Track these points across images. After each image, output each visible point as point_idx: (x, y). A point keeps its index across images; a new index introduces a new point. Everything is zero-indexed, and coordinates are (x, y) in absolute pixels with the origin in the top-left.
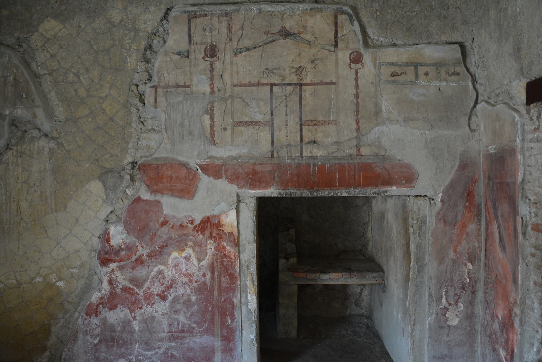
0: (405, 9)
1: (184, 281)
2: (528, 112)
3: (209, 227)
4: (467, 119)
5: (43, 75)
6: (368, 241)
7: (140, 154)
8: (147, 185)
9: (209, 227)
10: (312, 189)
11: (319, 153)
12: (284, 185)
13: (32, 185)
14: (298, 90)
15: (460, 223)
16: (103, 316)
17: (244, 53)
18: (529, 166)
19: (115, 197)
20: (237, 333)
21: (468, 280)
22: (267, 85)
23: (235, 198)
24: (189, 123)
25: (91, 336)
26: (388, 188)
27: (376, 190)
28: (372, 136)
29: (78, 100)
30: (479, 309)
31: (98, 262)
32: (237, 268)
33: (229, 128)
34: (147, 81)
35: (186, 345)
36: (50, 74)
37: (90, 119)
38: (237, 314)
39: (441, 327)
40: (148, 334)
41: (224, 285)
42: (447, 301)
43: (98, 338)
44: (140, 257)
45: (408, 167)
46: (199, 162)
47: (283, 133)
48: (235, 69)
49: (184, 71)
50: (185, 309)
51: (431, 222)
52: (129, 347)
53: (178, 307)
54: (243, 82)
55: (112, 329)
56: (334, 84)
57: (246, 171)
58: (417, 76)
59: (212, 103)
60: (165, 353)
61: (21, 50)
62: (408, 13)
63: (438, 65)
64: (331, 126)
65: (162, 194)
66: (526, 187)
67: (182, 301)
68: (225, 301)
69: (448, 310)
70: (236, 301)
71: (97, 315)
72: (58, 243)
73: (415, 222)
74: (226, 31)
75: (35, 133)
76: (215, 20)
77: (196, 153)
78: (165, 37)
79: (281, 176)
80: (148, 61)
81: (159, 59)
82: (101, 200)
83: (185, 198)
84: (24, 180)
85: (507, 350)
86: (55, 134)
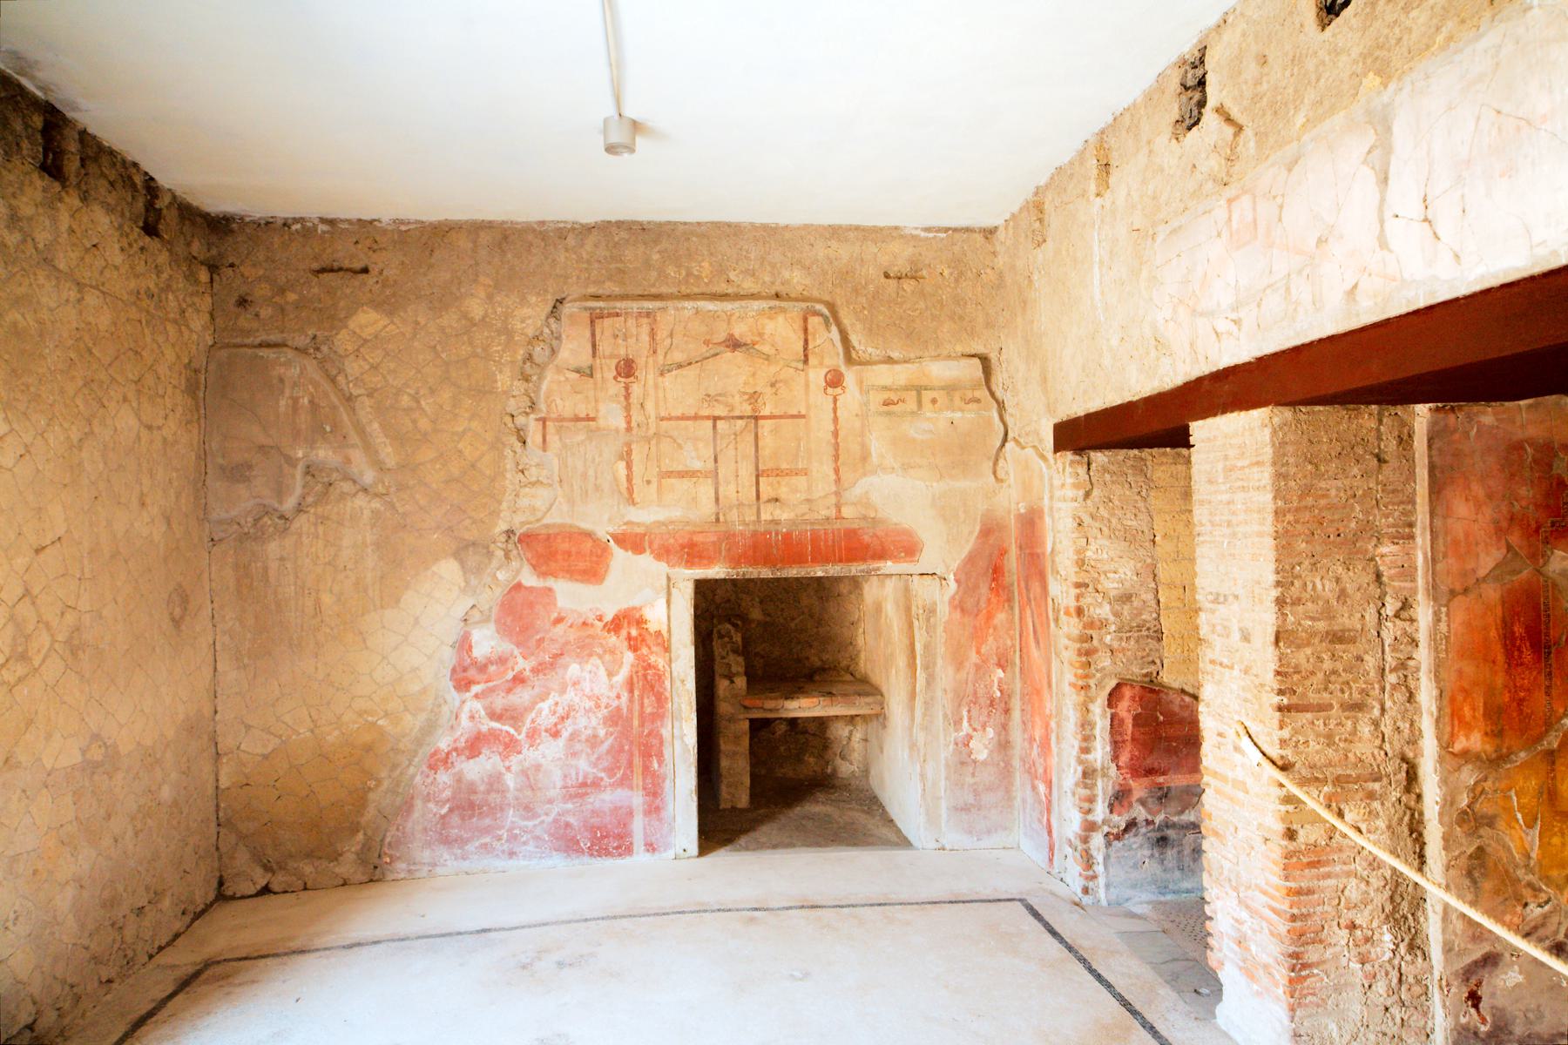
0: (904, 307)
1: (587, 707)
2: (1055, 460)
3: (626, 625)
4: (991, 464)
5: (360, 396)
6: (859, 651)
7: (518, 519)
8: (531, 564)
9: (626, 625)
10: (775, 566)
11: (784, 515)
12: (736, 561)
13: (341, 567)
14: (753, 425)
15: (984, 611)
16: (457, 769)
17: (674, 372)
18: (1059, 532)
19: (480, 583)
20: (668, 784)
21: (998, 694)
22: (708, 418)
23: (664, 582)
24: (596, 473)
25: (437, 803)
26: (880, 564)
27: (863, 567)
28: (857, 491)
29: (418, 437)
30: (1017, 735)
31: (451, 684)
32: (667, 683)
33: (655, 481)
34: (528, 410)
35: (589, 807)
36: (370, 395)
37: (438, 466)
38: (667, 752)
39: (962, 763)
40: (529, 793)
41: (648, 710)
42: (970, 725)
43: (448, 806)
44: (521, 672)
45: (908, 533)
46: (611, 530)
47: (732, 488)
48: (661, 395)
49: (587, 397)
50: (589, 750)
51: (943, 610)
52: (498, 815)
53: (578, 747)
54: (673, 415)
55: (472, 789)
56: (803, 417)
57: (681, 541)
58: (920, 403)
59: (628, 445)
60: (556, 821)
61: (319, 356)
62: (909, 312)
63: (950, 388)
64: (799, 477)
65: (556, 577)
66: (1057, 559)
67: (583, 737)
68: (649, 734)
69: (971, 738)
70: (665, 733)
71: (447, 769)
72: (384, 658)
73: (921, 611)
74: (647, 339)
75: (347, 487)
76: (631, 322)
77: (606, 517)
78: (555, 343)
79: (729, 549)
80: (527, 379)
81: (549, 378)
82: (457, 588)
83: (591, 583)
84: (327, 560)
85: (1045, 782)
86: (381, 489)
